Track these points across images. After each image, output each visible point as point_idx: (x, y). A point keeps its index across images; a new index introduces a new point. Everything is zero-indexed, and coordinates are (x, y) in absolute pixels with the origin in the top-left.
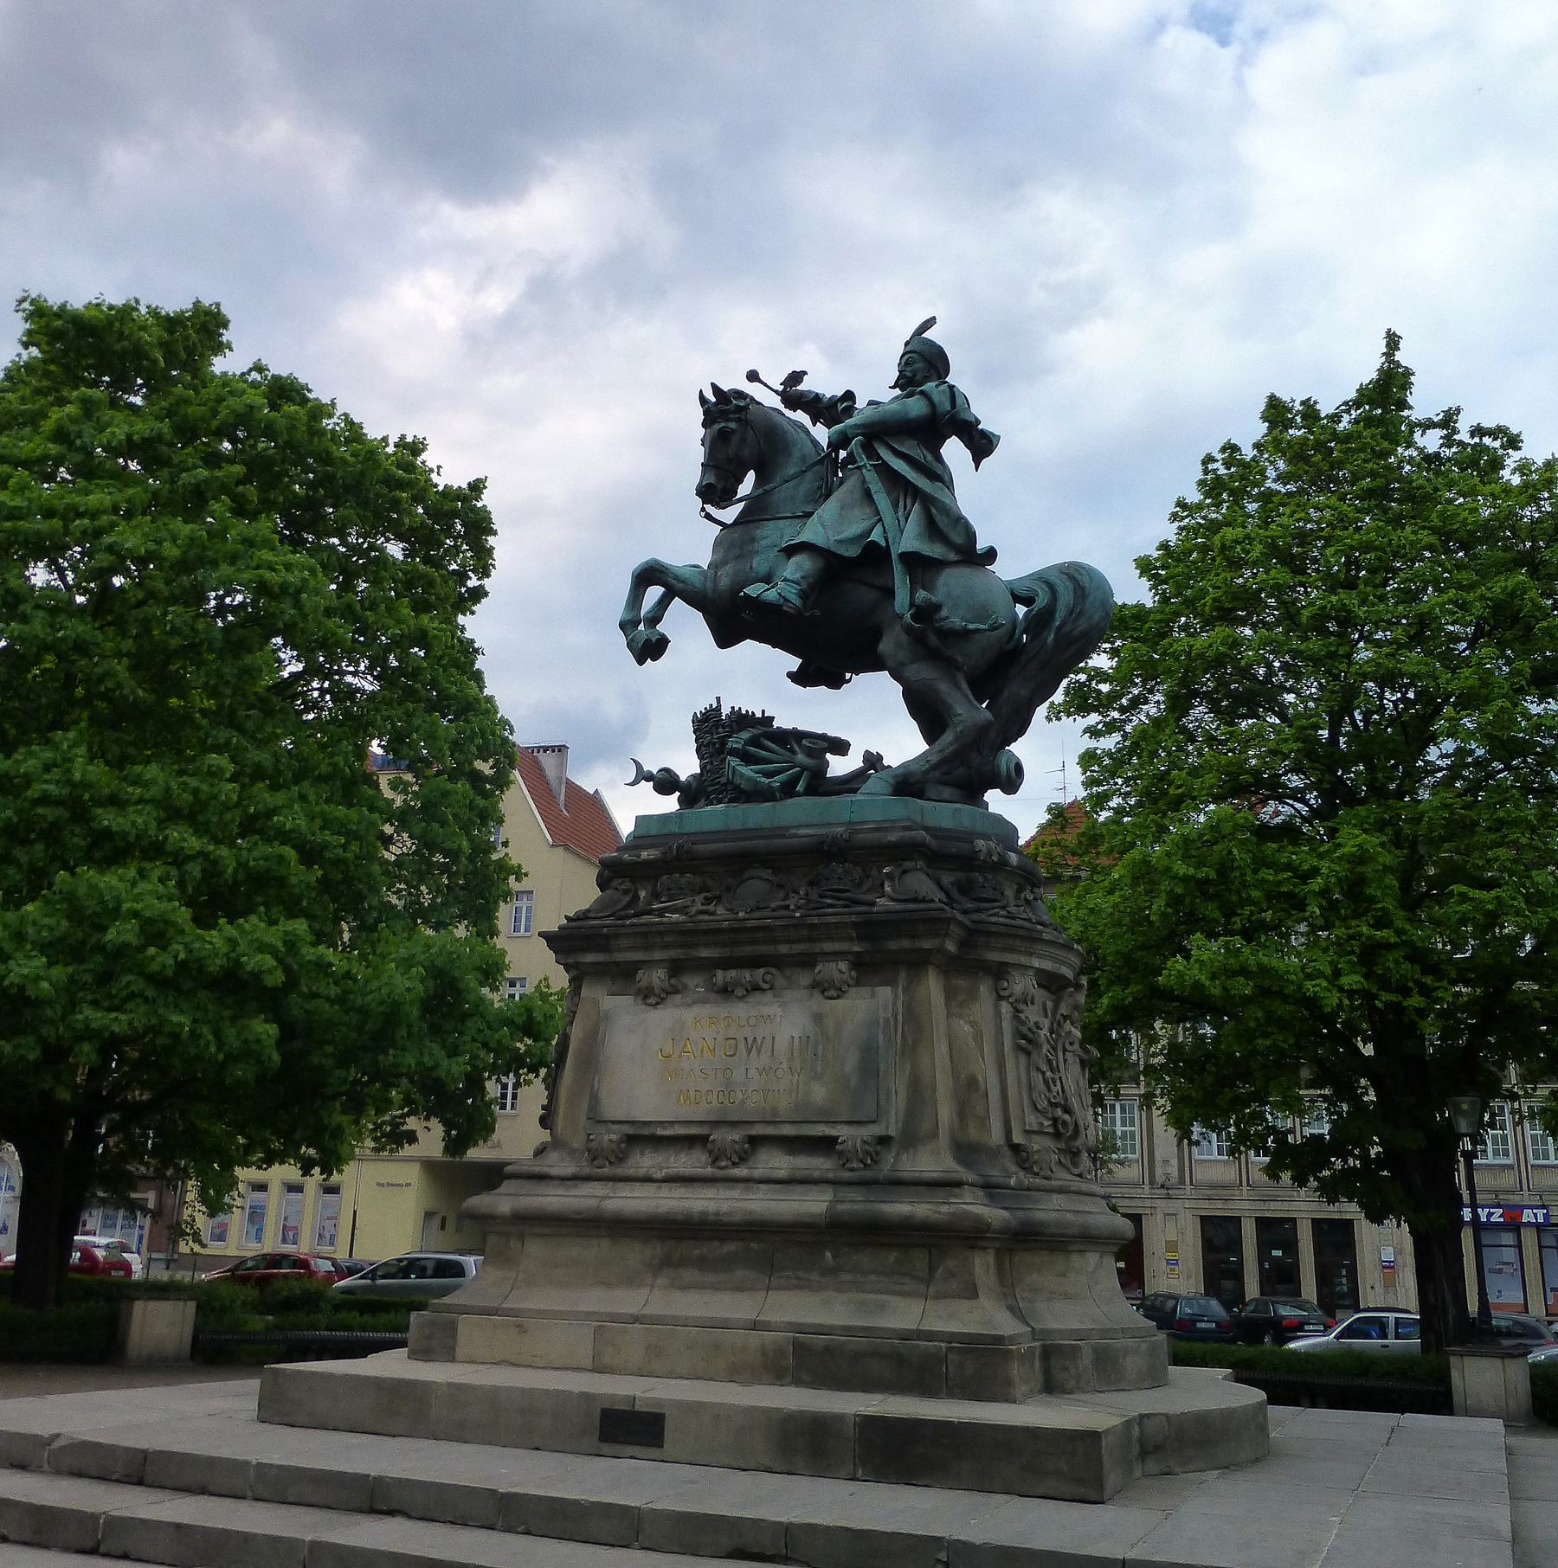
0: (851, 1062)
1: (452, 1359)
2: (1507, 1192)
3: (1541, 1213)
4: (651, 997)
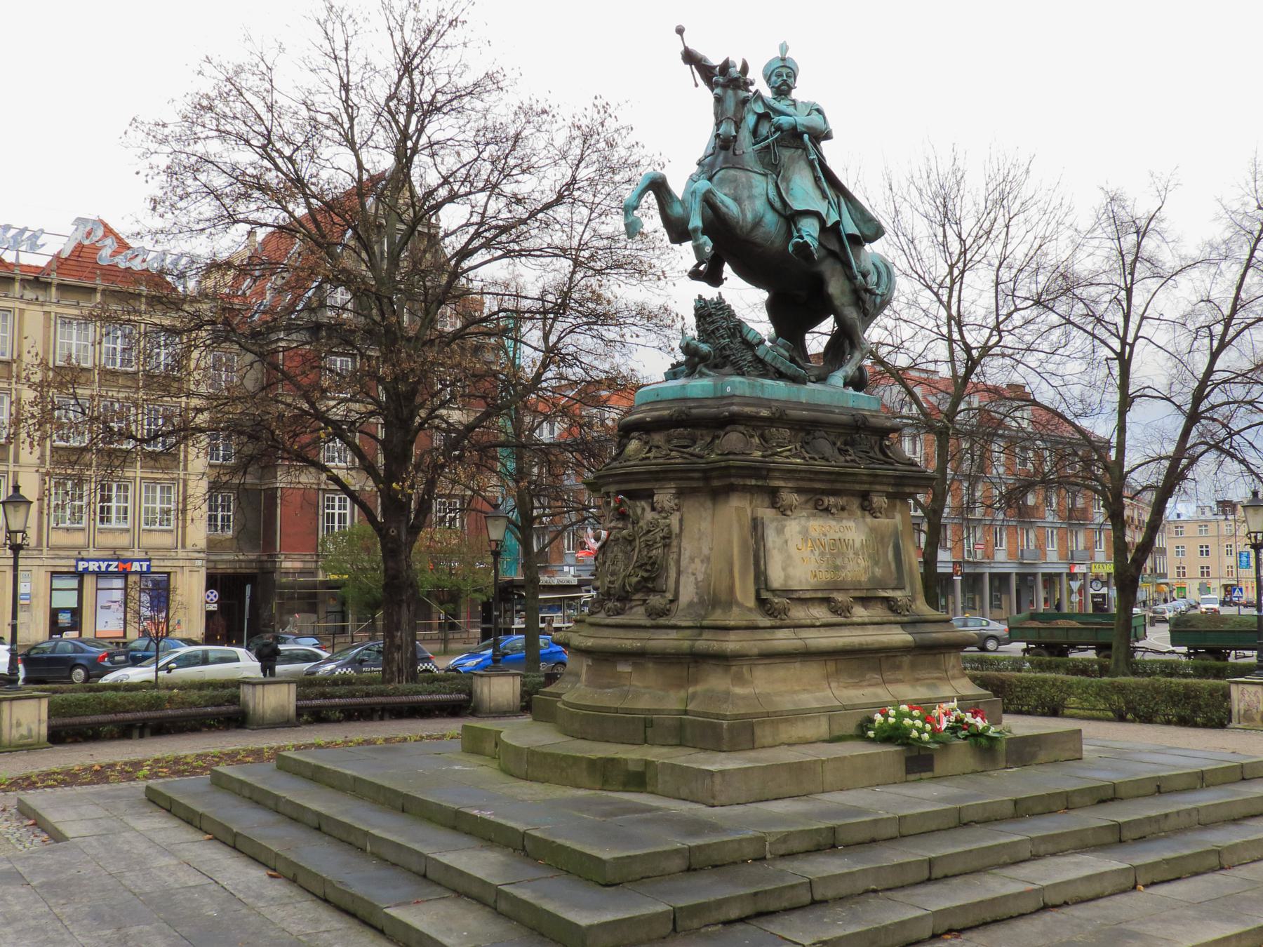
2: (123, 549)
3: (145, 564)
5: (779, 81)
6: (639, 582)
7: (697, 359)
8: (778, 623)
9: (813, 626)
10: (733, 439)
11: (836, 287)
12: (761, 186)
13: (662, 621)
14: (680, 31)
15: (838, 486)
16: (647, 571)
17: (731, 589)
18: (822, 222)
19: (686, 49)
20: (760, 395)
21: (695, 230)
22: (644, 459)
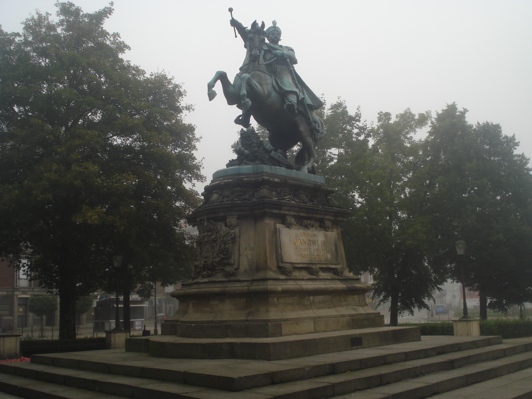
0: (333, 248)
1: (281, 335)
4: (289, 226)
5: (273, 37)
6: (220, 261)
7: (243, 157)
8: (288, 277)
9: (303, 280)
10: (264, 191)
11: (303, 128)
12: (270, 80)
13: (233, 278)
14: (231, 10)
15: (311, 215)
16: (224, 255)
17: (266, 261)
18: (298, 97)
19: (233, 18)
20: (274, 172)
21: (244, 95)
22: (221, 202)
